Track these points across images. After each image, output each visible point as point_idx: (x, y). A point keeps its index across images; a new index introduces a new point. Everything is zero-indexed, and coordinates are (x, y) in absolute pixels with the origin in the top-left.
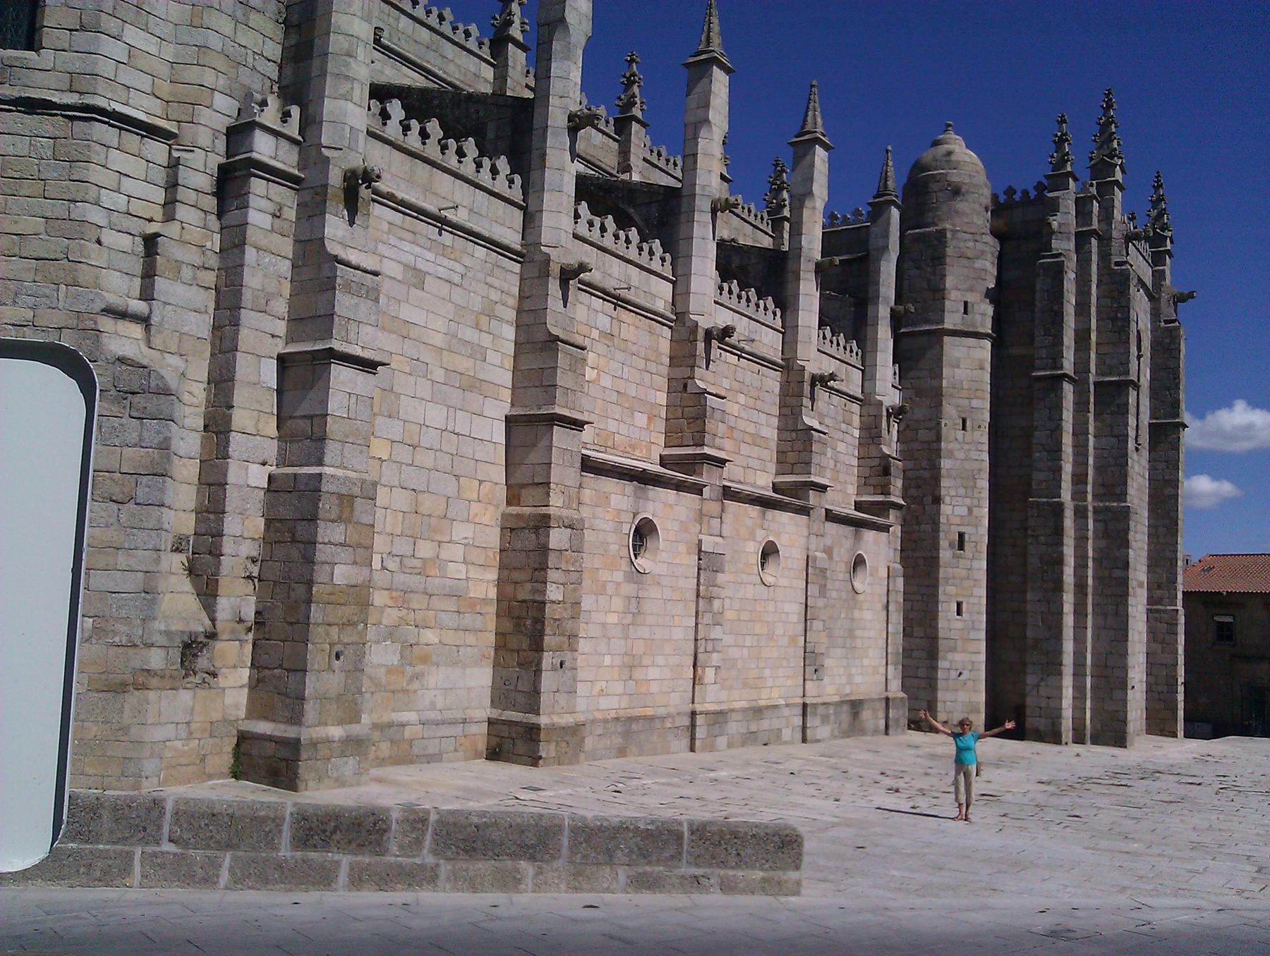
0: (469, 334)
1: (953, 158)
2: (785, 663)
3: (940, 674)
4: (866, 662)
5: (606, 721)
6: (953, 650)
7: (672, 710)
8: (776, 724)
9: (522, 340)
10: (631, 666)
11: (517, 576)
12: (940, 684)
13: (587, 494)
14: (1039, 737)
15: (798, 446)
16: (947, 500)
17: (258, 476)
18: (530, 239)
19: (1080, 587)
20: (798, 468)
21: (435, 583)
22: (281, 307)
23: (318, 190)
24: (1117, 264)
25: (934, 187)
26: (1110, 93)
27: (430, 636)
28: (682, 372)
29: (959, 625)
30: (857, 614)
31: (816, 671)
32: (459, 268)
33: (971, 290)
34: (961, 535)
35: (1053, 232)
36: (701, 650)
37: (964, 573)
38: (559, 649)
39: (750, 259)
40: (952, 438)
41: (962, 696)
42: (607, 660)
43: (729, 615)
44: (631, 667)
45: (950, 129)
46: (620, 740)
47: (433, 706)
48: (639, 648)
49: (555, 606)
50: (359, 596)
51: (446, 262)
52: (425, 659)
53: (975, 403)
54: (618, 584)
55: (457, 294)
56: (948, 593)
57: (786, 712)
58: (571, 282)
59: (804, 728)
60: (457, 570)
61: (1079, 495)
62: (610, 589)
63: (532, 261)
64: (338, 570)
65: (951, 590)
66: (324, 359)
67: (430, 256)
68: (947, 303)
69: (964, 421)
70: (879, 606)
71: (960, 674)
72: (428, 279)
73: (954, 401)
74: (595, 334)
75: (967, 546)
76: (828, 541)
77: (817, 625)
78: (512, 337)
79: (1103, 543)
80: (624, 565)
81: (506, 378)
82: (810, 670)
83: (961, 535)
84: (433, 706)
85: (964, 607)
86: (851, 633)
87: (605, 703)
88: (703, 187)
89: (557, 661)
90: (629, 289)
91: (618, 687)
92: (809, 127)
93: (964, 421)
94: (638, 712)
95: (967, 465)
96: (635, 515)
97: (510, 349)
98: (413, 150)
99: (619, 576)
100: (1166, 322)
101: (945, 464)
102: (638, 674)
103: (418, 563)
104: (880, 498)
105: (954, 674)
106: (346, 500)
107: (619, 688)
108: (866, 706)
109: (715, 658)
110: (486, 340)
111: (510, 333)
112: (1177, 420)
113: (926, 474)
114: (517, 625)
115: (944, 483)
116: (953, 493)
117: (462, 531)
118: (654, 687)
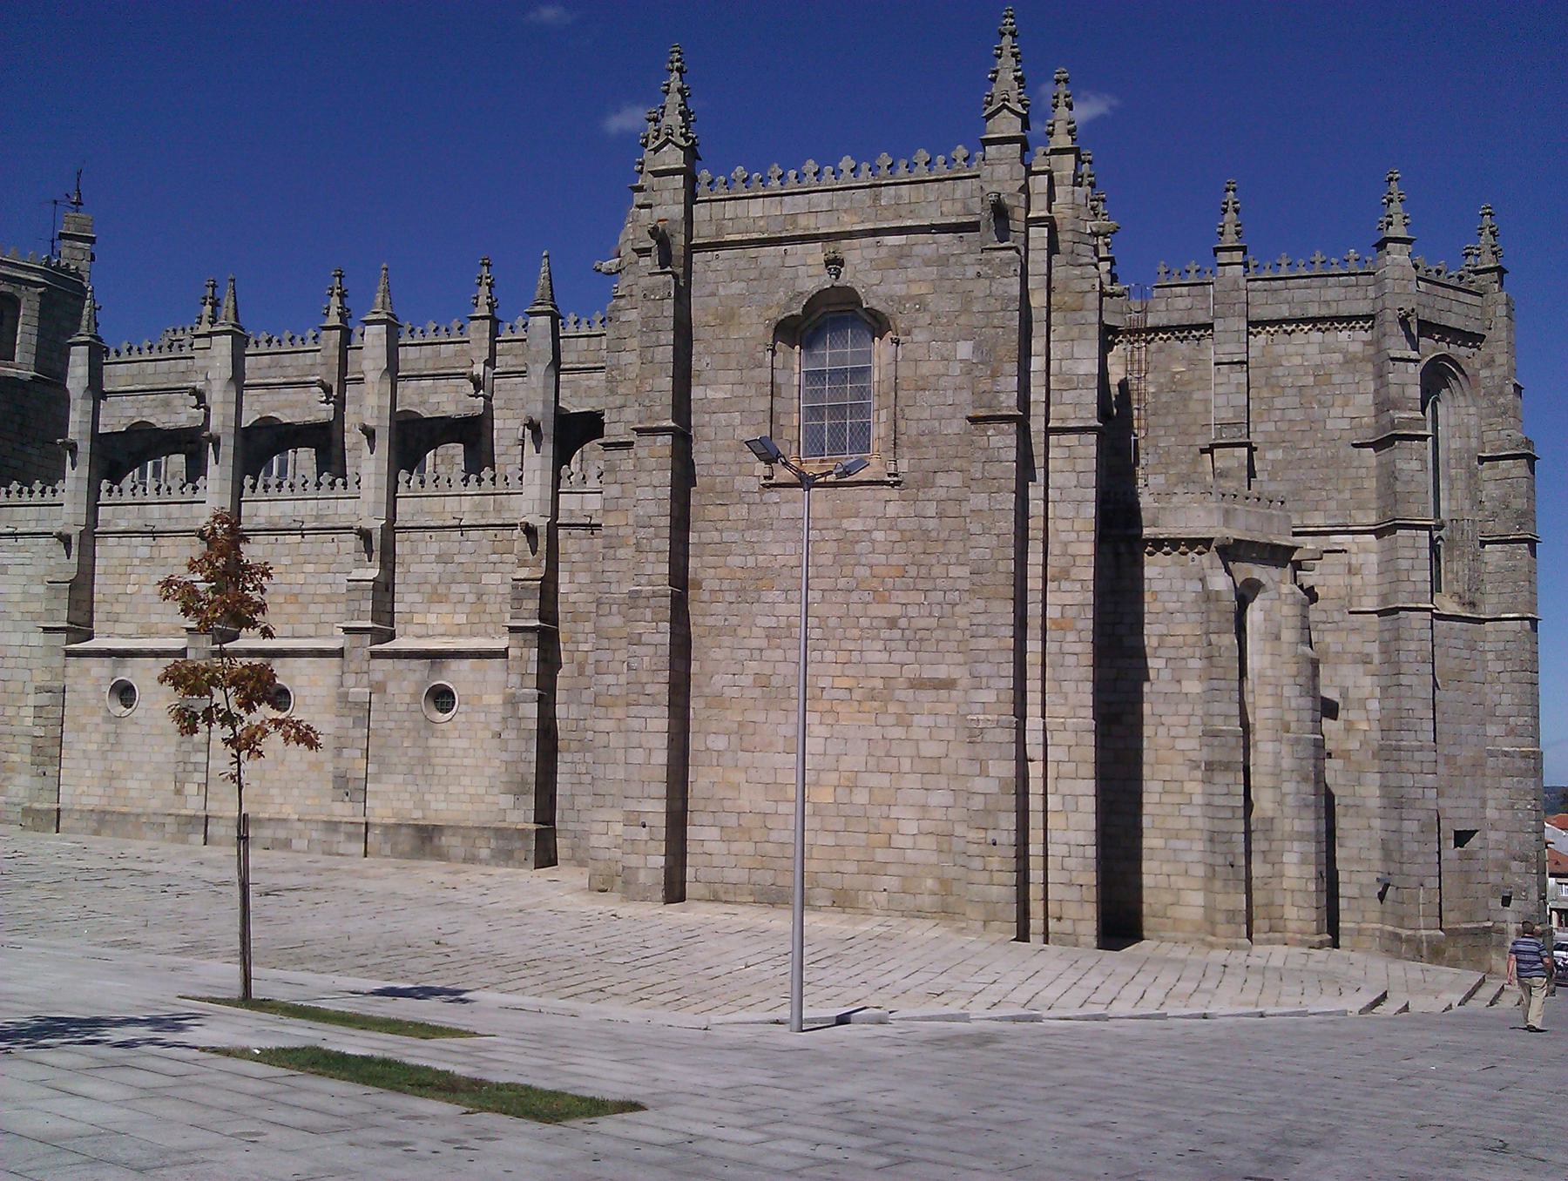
2: (301, 784)
4: (452, 789)
5: (81, 811)
7: (150, 810)
8: (282, 834)
10: (111, 777)
13: (70, 671)
21: (16, 729)
27: (15, 757)
30: (433, 742)
32: (28, 555)
38: (43, 764)
42: (88, 773)
44: (111, 779)
46: (95, 824)
47: (17, 795)
48: (116, 767)
51: (20, 554)
52: (12, 770)
54: (98, 725)
55: (29, 570)
57: (300, 825)
62: (89, 728)
74: (136, 562)
76: (378, 676)
80: (103, 713)
84: (17, 795)
86: (425, 761)
87: (84, 800)
91: (100, 792)
94: (117, 809)
99: (98, 719)
102: (116, 783)
107: (100, 792)
108: (448, 832)
118: (133, 793)
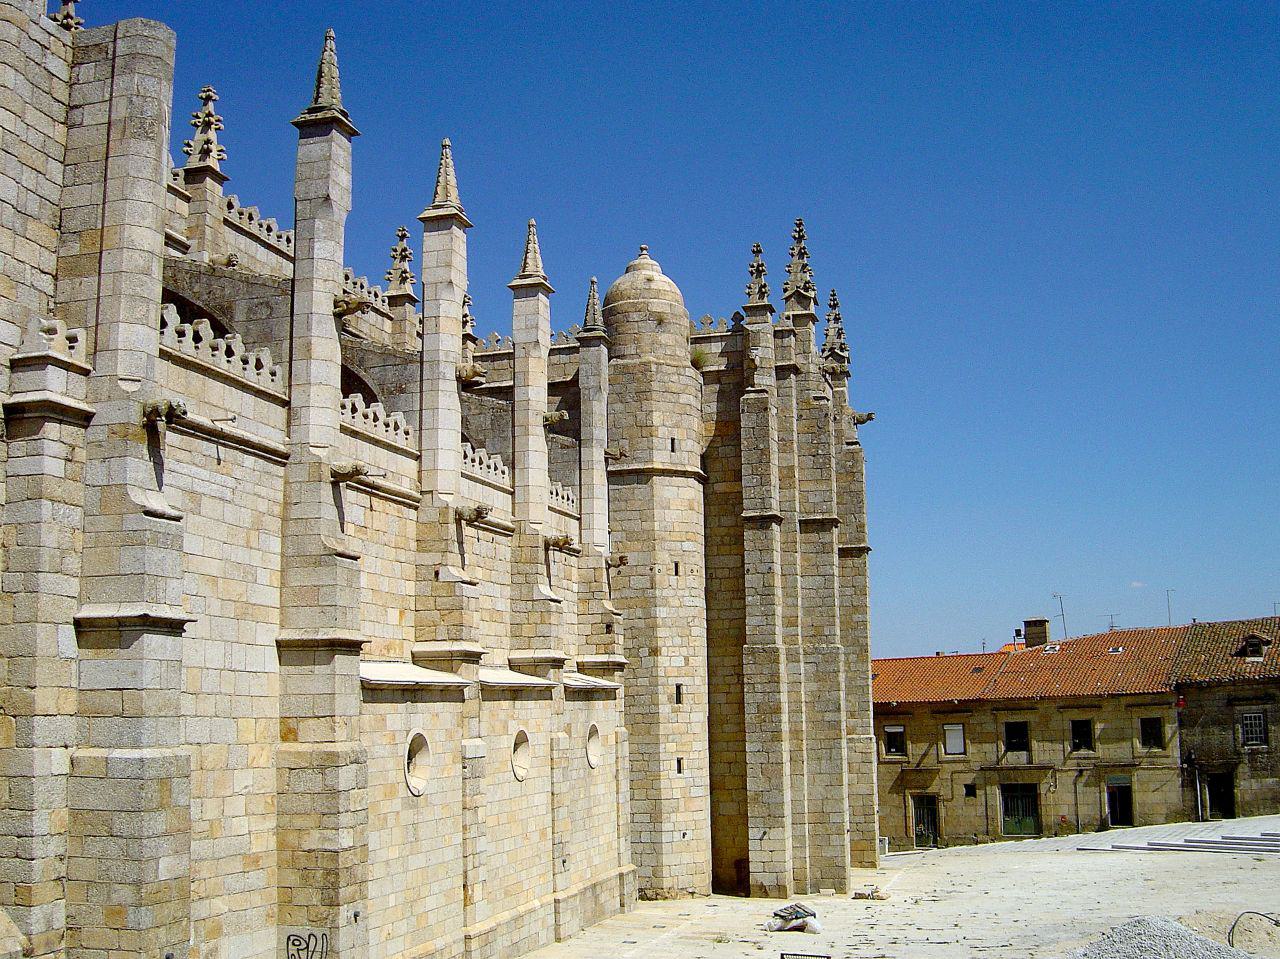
0: (241, 555)
1: (653, 286)
3: (665, 838)
6: (676, 810)
9: (290, 552)
11: (299, 822)
12: (666, 848)
14: (764, 892)
15: (535, 617)
16: (664, 650)
17: (59, 761)
18: (296, 437)
19: (796, 733)
20: (536, 642)
22: (73, 563)
23: (116, 428)
24: (816, 398)
25: (635, 316)
26: (801, 224)
28: (430, 559)
29: (682, 783)
31: (564, 862)
32: (231, 483)
33: (677, 426)
34: (678, 687)
35: (756, 368)
36: (470, 867)
37: (683, 728)
39: (470, 409)
40: (666, 584)
41: (686, 858)
43: (491, 822)
45: (645, 252)
49: (347, 854)
50: (182, 889)
51: (219, 478)
53: (687, 546)
54: (398, 813)
56: (668, 750)
58: (341, 484)
59: (557, 925)
60: (242, 825)
61: (790, 639)
62: (391, 821)
63: (300, 463)
64: (163, 863)
65: (671, 747)
66: (135, 626)
67: (204, 474)
68: (655, 440)
69: (676, 565)
70: (610, 777)
71: (684, 835)
72: (205, 500)
73: (667, 545)
75: (684, 698)
77: (563, 812)
78: (278, 550)
79: (814, 686)
81: (273, 597)
82: (559, 862)
83: (678, 687)
85: (684, 763)
88: (447, 353)
89: (351, 914)
90: (384, 476)
92: (530, 270)
93: (676, 565)
95: (682, 612)
96: (408, 732)
97: (276, 562)
98: (190, 358)
100: (848, 444)
101: (661, 612)
102: (419, 909)
103: (205, 826)
104: (604, 658)
105: (677, 836)
106: (164, 781)
109: (482, 873)
110: (256, 558)
111: (276, 545)
112: (862, 545)
113: (641, 624)
114: (302, 877)
115: (661, 632)
116: (669, 643)
117: (243, 780)
